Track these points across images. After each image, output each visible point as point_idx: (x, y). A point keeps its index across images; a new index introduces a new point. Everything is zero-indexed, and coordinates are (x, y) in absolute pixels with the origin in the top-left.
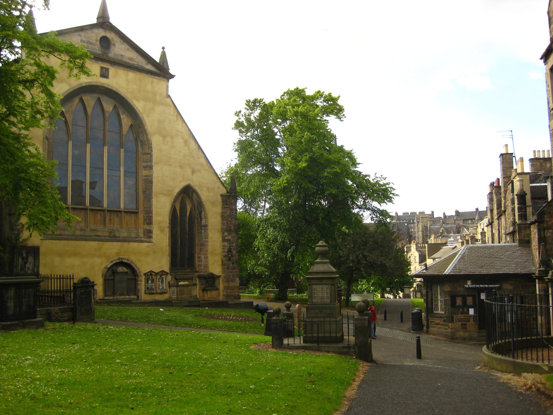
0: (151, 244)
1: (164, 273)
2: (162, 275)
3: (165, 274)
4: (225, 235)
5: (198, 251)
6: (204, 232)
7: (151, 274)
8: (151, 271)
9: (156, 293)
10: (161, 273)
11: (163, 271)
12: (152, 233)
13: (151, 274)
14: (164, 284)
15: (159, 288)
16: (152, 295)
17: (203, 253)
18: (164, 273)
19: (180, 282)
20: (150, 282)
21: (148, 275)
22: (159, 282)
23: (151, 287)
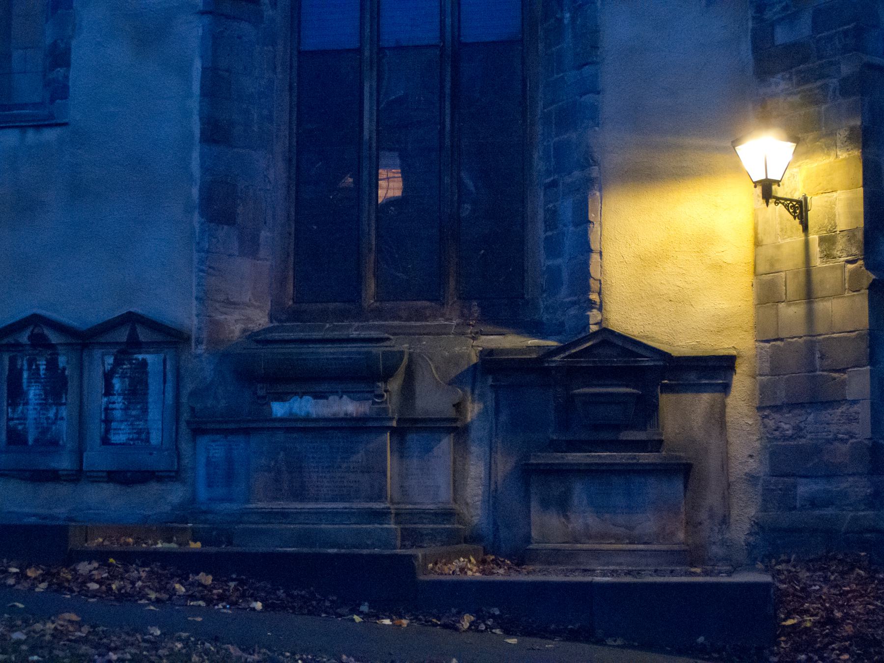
0: (50, 135)
1: (144, 335)
2: (134, 344)
3: (157, 337)
4: (768, 15)
5: (549, 173)
6: (573, 19)
7: (39, 342)
8: (35, 320)
9: (77, 476)
10: (122, 335)
11: (131, 319)
12: (68, 65)
13: (43, 337)
14: (154, 413)
15: (105, 441)
16: (47, 490)
17: (568, 180)
18: (144, 335)
19: (281, 397)
20: (33, 393)
21: (17, 345)
22: (109, 391)
23: (45, 431)
